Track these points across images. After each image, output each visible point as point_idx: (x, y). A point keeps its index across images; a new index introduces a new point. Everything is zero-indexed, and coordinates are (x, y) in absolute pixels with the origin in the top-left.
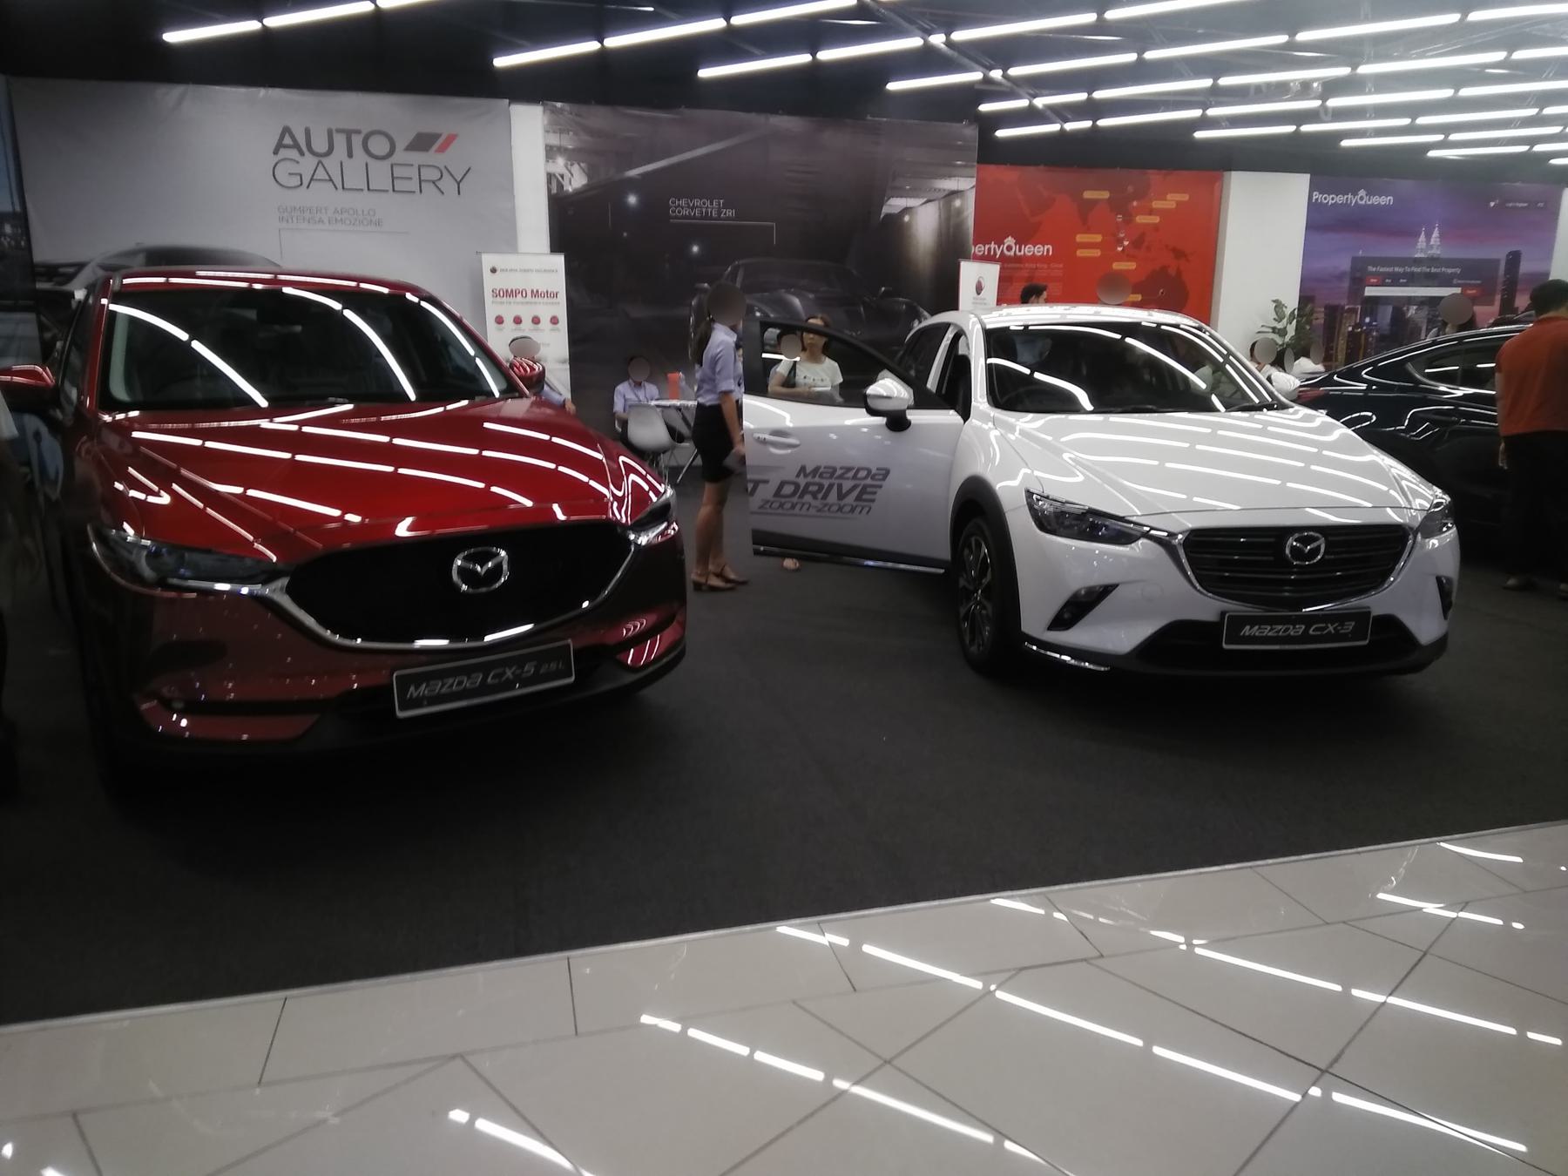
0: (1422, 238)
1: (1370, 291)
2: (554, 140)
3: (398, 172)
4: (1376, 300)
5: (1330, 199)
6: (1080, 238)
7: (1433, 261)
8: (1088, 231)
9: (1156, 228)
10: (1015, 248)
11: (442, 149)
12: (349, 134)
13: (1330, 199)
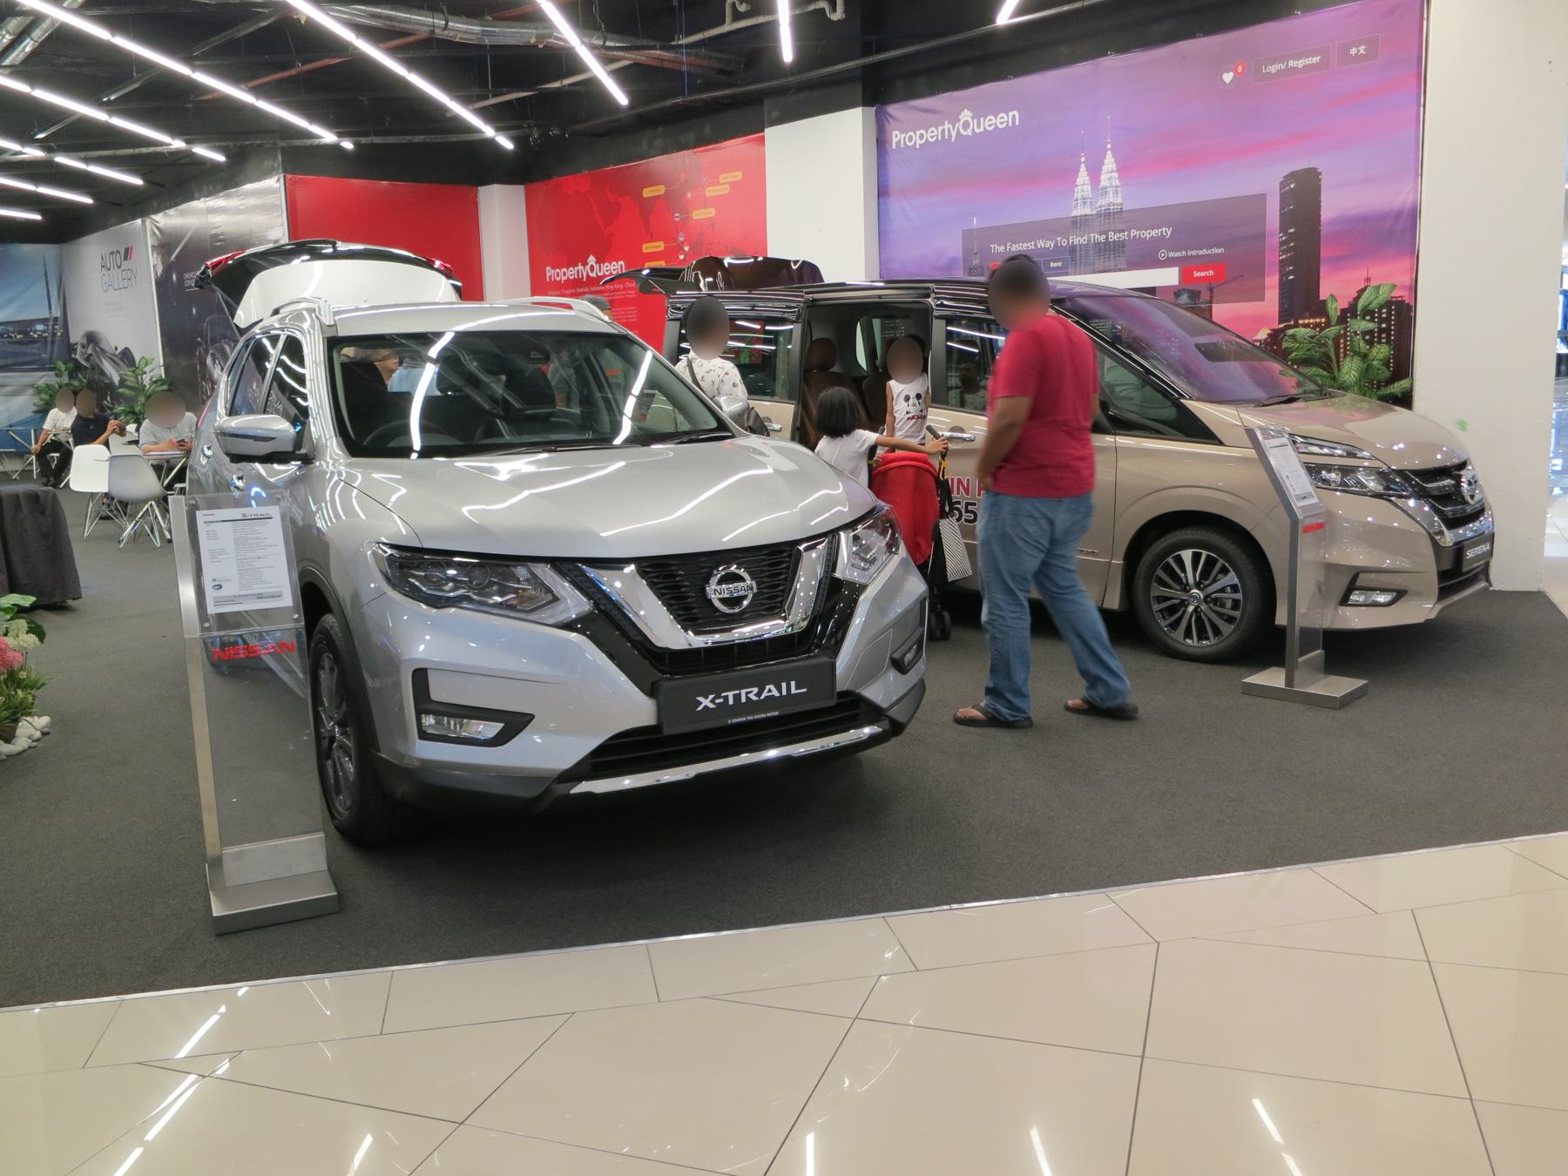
0: (1083, 177)
7: (1109, 216)
8: (652, 239)
9: (711, 222)
10: (596, 267)
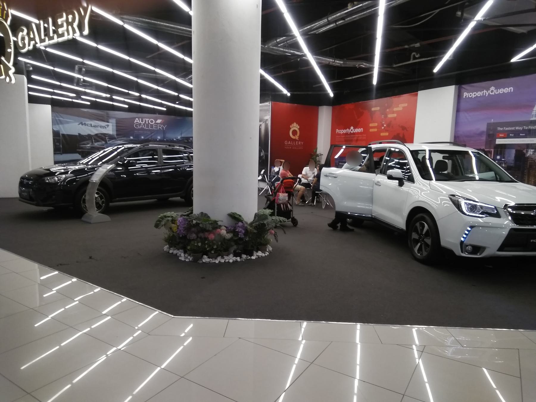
1: (499, 141)
4: (503, 147)
6: (371, 125)
8: (374, 122)
9: (395, 119)
10: (353, 130)
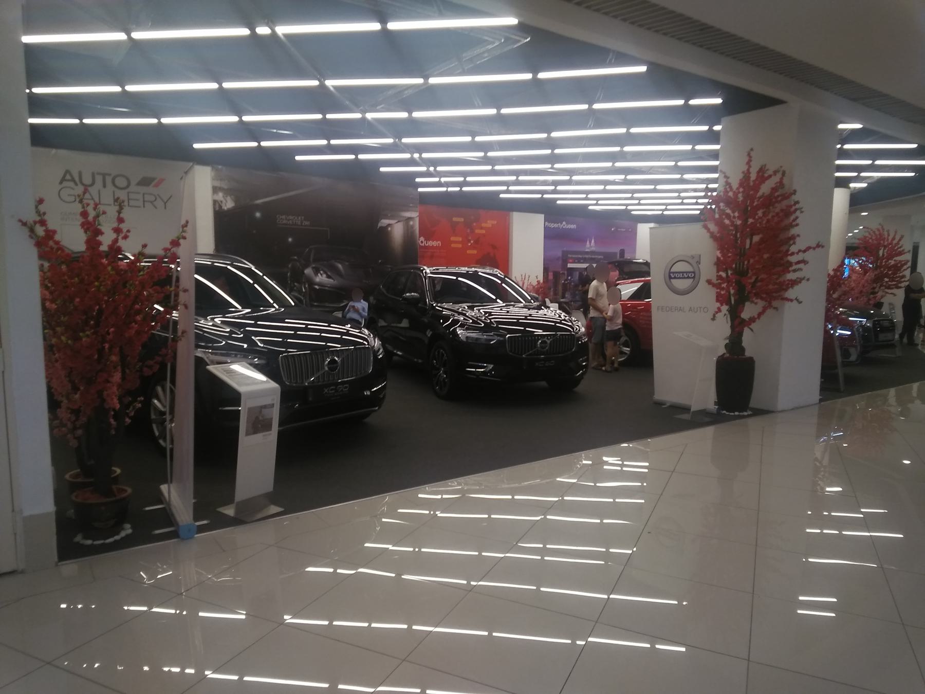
1: (570, 265)
2: (217, 184)
3: (132, 196)
5: (552, 225)
6: (453, 239)
7: (593, 253)
8: (456, 236)
9: (484, 235)
11: (157, 185)
12: (104, 175)
13: (552, 225)
